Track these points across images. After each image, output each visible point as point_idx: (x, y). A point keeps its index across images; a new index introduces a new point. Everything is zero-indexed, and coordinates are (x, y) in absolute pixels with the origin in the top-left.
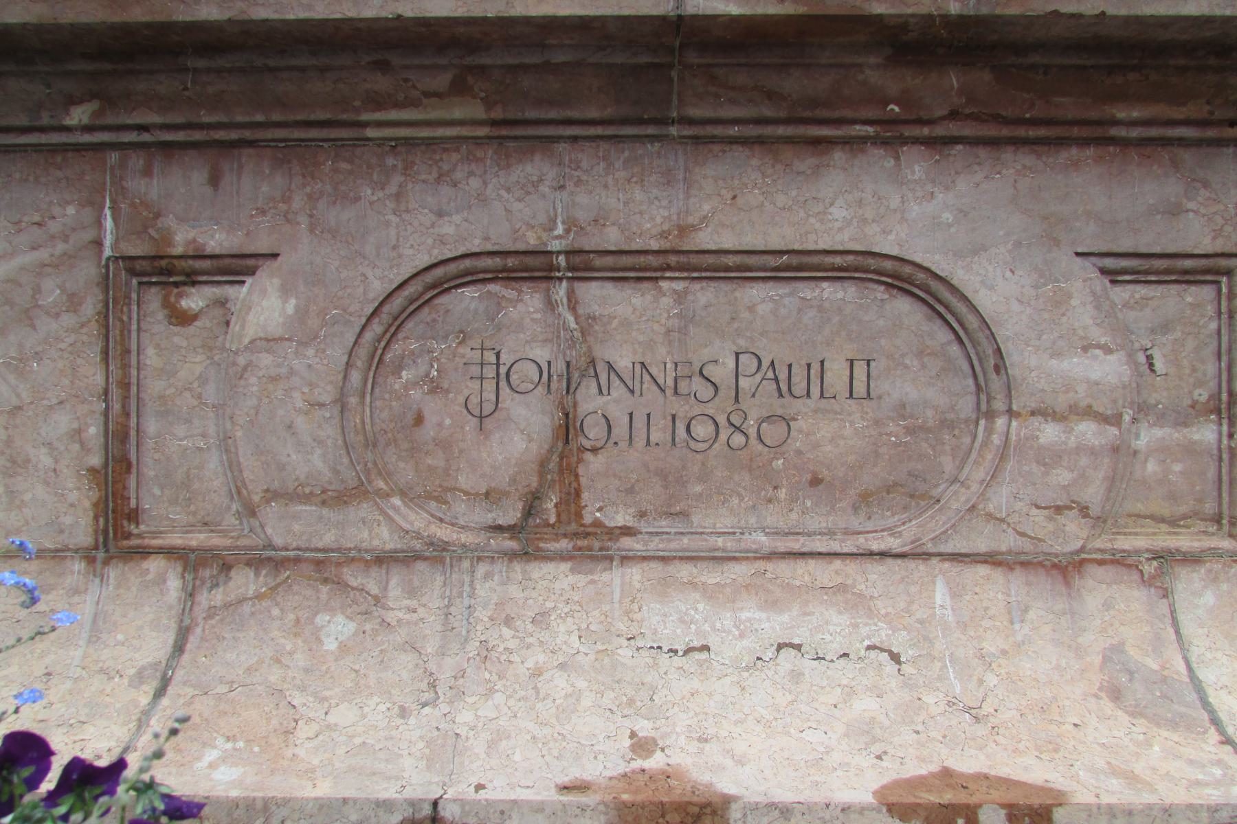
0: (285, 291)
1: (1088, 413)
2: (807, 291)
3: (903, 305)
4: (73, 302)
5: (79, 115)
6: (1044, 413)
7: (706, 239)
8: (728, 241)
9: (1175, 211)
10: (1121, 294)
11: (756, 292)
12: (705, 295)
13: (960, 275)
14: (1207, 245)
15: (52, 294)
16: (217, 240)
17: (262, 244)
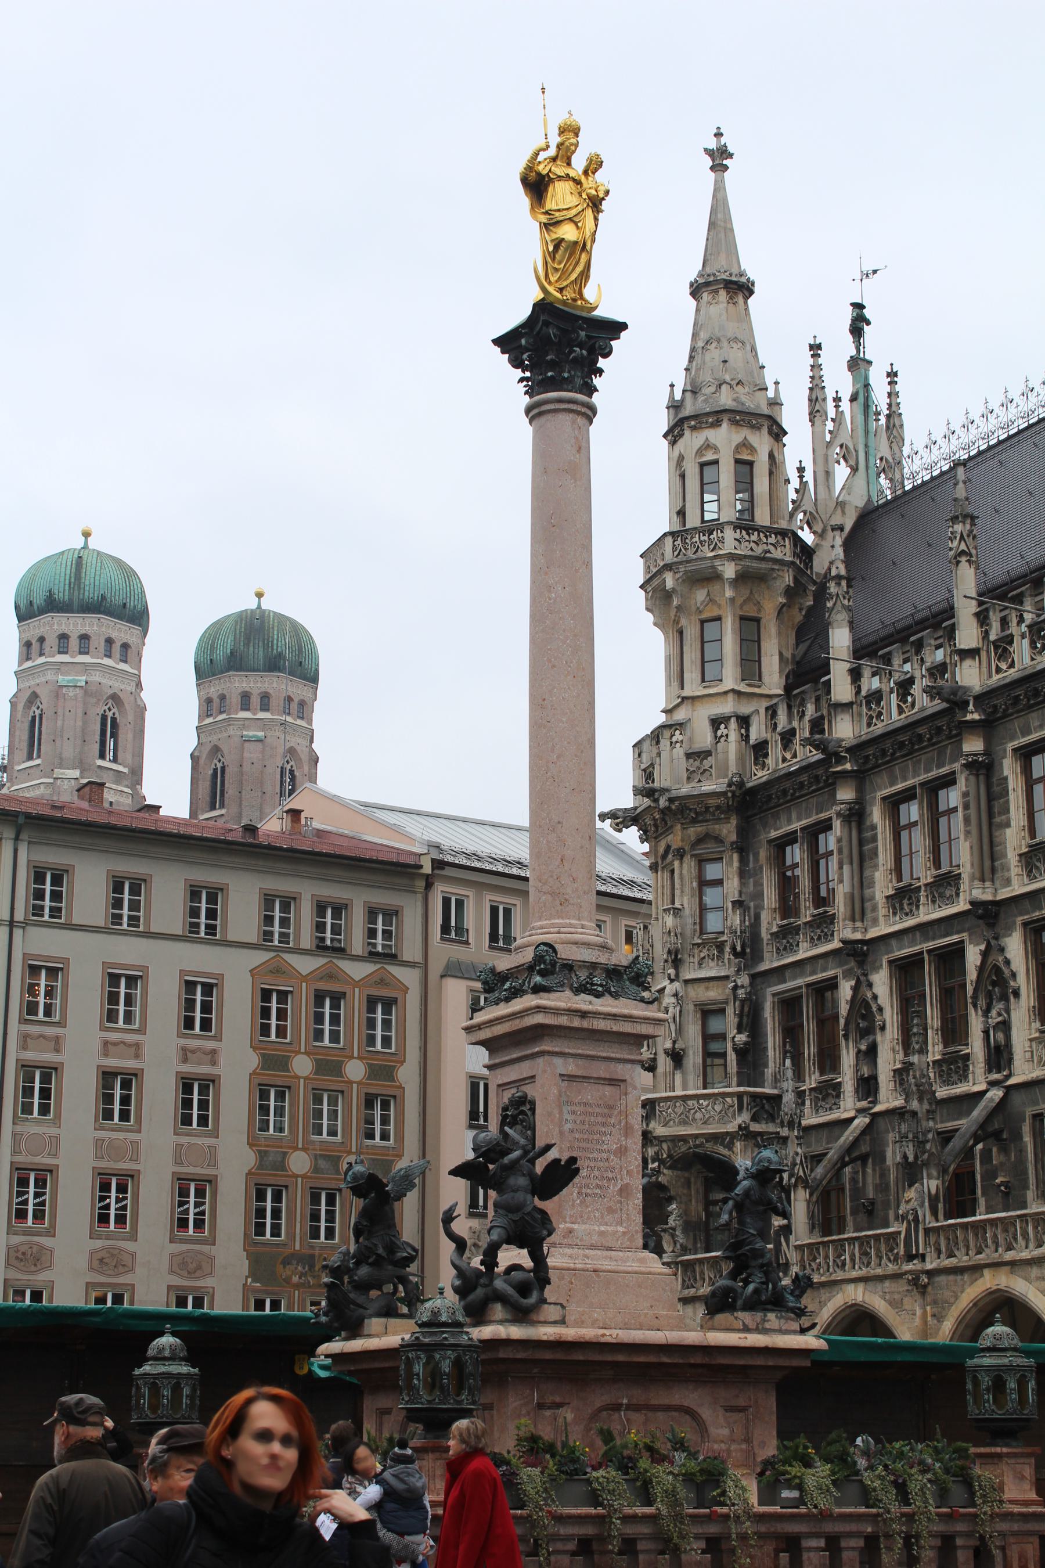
0: (572, 1412)
1: (722, 1442)
2: (670, 1414)
3: (687, 1417)
4: (528, 1414)
5: (536, 1370)
6: (715, 1442)
7: (654, 1402)
8: (656, 1403)
9: (737, 1396)
10: (728, 1414)
11: (659, 1414)
12: (650, 1414)
13: (699, 1411)
14: (743, 1404)
15: (524, 1412)
16: (558, 1399)
17: (567, 1401)
